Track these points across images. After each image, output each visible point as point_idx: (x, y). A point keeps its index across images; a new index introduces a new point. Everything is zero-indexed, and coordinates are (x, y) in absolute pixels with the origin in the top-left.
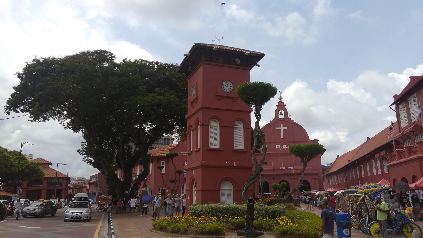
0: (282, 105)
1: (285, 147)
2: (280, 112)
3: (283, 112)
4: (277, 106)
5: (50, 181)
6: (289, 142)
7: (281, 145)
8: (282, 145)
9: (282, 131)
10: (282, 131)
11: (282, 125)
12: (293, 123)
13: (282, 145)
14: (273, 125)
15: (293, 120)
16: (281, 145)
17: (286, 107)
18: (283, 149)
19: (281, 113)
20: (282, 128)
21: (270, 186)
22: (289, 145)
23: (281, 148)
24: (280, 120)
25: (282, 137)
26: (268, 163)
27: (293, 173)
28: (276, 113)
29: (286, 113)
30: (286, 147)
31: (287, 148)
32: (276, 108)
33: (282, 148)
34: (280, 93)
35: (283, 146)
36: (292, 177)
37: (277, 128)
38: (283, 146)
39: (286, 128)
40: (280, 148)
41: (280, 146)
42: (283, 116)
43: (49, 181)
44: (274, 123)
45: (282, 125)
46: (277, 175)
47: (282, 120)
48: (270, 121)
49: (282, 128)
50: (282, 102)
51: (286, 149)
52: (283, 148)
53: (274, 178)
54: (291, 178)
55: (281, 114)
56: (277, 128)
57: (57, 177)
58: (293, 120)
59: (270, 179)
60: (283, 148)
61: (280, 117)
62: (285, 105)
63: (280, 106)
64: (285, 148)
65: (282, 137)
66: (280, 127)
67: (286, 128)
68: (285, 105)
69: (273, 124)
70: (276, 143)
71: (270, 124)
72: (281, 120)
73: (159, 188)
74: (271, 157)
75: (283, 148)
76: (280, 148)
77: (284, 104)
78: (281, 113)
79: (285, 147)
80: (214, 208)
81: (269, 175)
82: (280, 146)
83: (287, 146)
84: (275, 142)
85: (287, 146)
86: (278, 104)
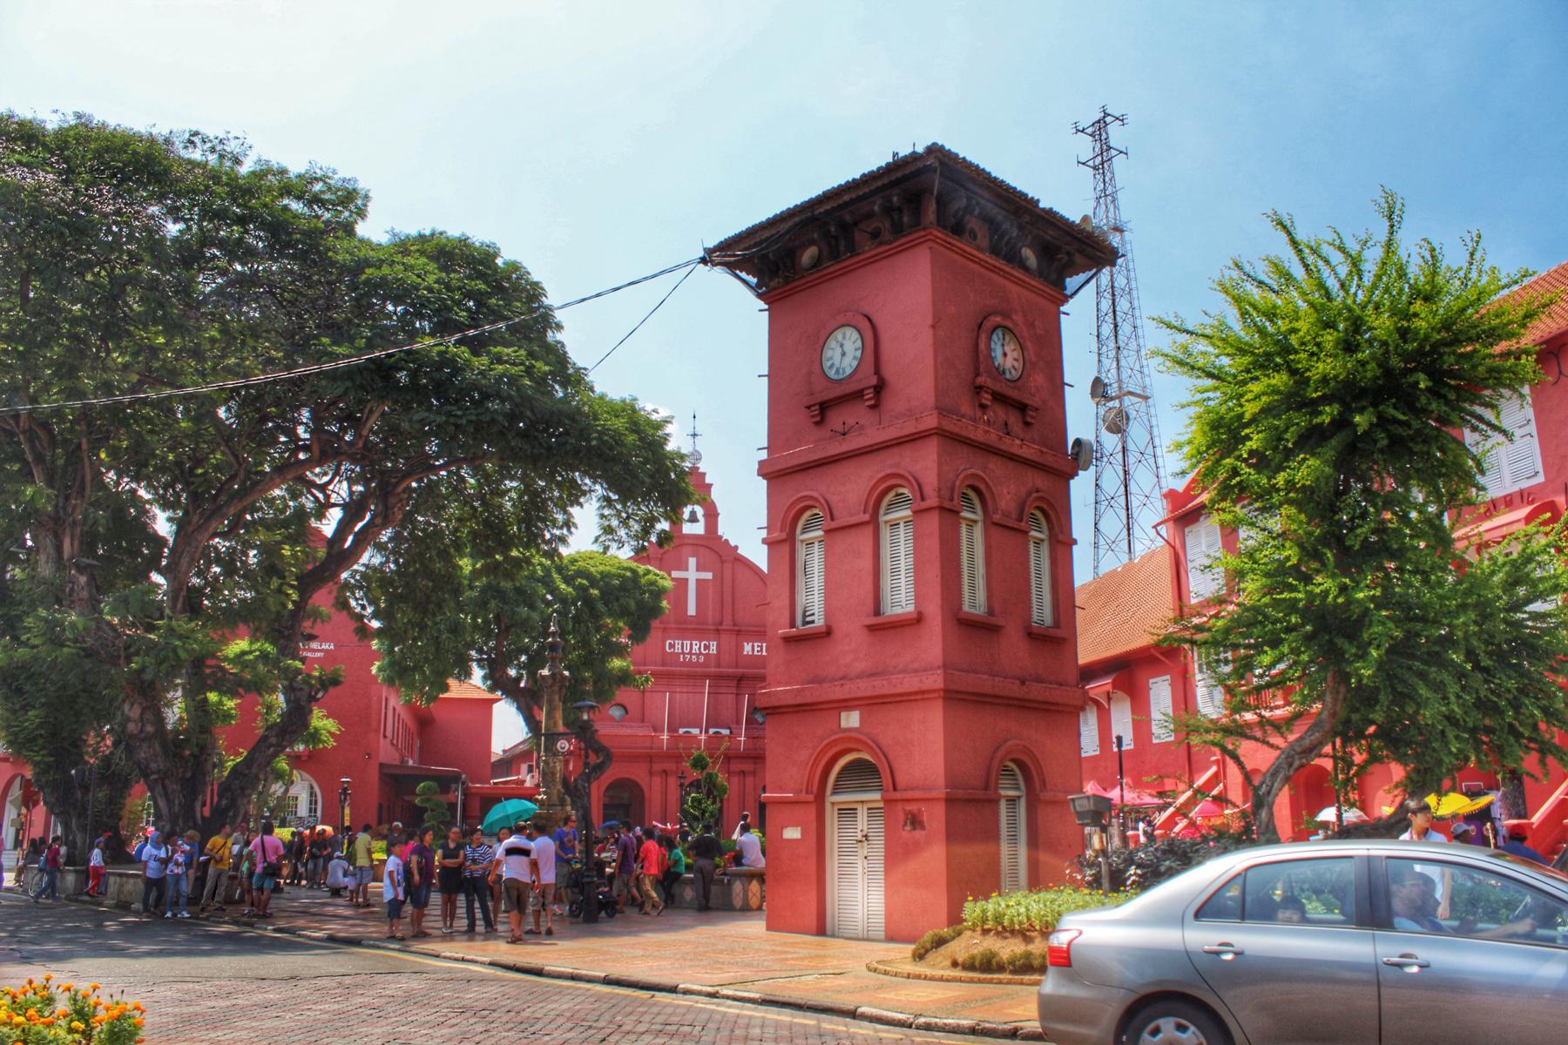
3: (700, 511)
6: (717, 632)
11: (692, 562)
17: (715, 495)
19: (693, 513)
20: (692, 574)
23: (683, 653)
24: (686, 541)
25: (692, 610)
29: (712, 515)
33: (690, 653)
34: (694, 435)
39: (708, 576)
45: (692, 562)
47: (696, 542)
49: (692, 574)
50: (701, 470)
51: (702, 658)
62: (710, 486)
64: (701, 653)
65: (692, 610)
67: (708, 576)
68: (710, 486)
72: (691, 541)
78: (693, 513)
80: (1179, 846)
83: (707, 647)
85: (707, 647)
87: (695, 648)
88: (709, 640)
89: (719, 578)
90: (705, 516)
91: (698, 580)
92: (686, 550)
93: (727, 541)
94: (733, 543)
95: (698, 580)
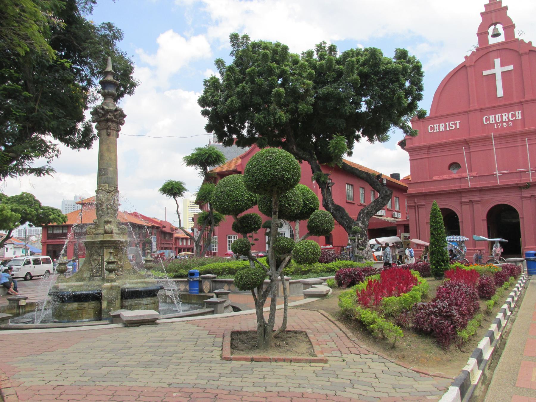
0: (496, 11)
1: (508, 118)
2: (491, 31)
3: (500, 27)
4: (482, 14)
5: (51, 232)
7: (497, 115)
8: (500, 115)
9: (499, 78)
10: (499, 78)
11: (497, 62)
12: (530, 51)
13: (500, 115)
14: (474, 66)
15: (530, 43)
16: (497, 115)
17: (510, 13)
18: (502, 125)
21: (462, 221)
22: (520, 112)
24: (491, 49)
25: (500, 93)
26: (461, 165)
27: (528, 182)
28: (482, 34)
29: (510, 27)
30: (511, 119)
31: (515, 119)
32: (480, 20)
33: (502, 122)
35: (502, 116)
36: (526, 193)
37: (485, 73)
38: (502, 116)
39: (511, 67)
40: (494, 122)
41: (495, 117)
42: (501, 39)
43: (49, 232)
44: (474, 61)
45: (497, 62)
46: (481, 190)
47: (498, 48)
48: (466, 57)
51: (511, 124)
52: (504, 120)
53: (472, 200)
54: (523, 196)
55: (496, 35)
56: (485, 73)
57: (83, 223)
58: (530, 43)
59: (461, 203)
60: (504, 122)
61: (492, 41)
62: (506, 8)
63: (491, 12)
64: (509, 121)
65: (500, 93)
66: (494, 67)
67: (511, 67)
68: (506, 8)
69: (473, 64)
70: (483, 111)
71: (465, 65)
72: (495, 48)
73: (227, 235)
74: (470, 150)
75: (504, 120)
76: (494, 122)
77: (503, 5)
79: (508, 118)
81: (459, 193)
82: (495, 117)
83: (513, 116)
84: (481, 109)
86: (483, 10)
87: (505, 118)
88: (515, 111)
89: (519, 68)
90: (504, 28)
91: (503, 73)
92: (491, 55)
93: (522, 41)
94: (527, 41)
95: (503, 73)
